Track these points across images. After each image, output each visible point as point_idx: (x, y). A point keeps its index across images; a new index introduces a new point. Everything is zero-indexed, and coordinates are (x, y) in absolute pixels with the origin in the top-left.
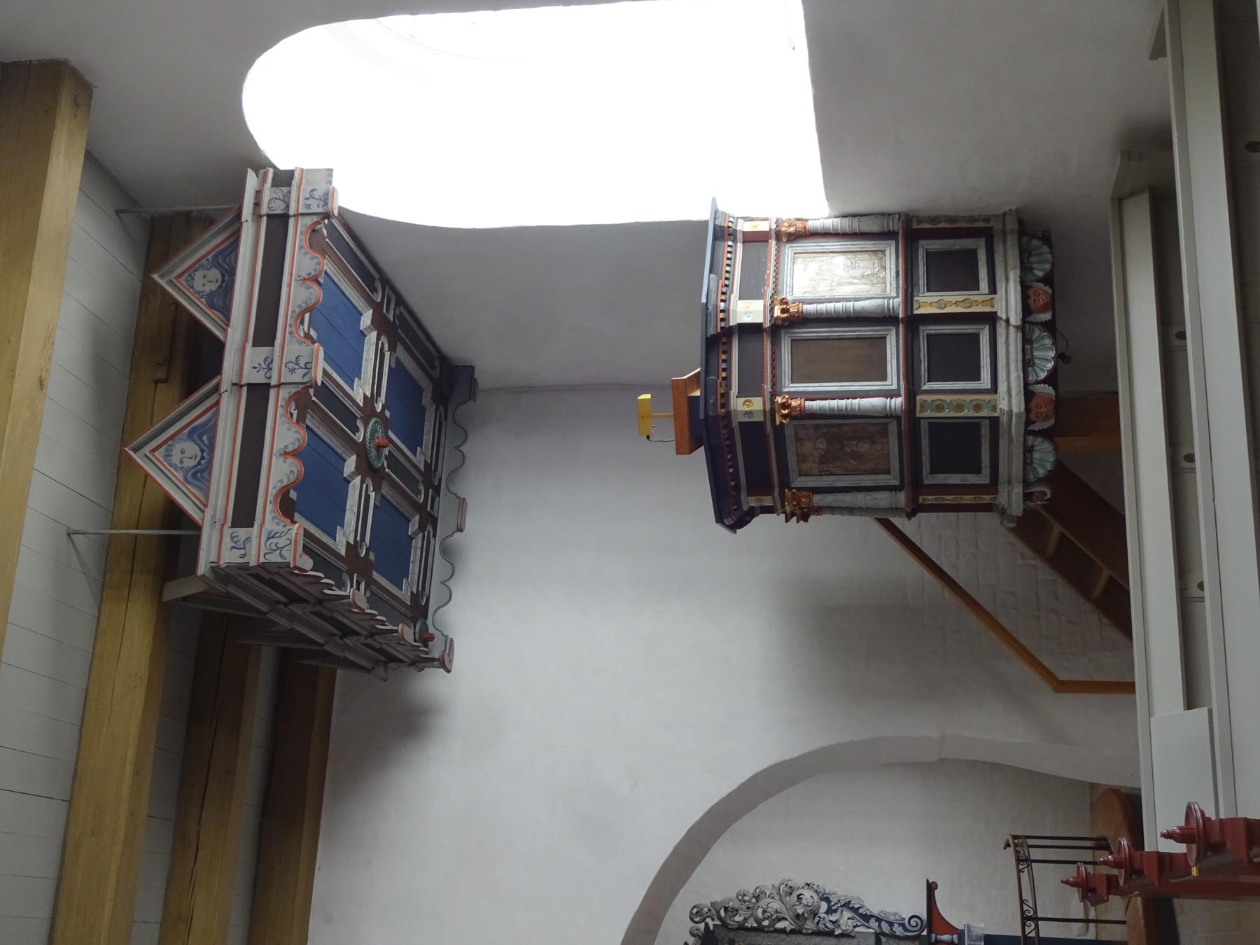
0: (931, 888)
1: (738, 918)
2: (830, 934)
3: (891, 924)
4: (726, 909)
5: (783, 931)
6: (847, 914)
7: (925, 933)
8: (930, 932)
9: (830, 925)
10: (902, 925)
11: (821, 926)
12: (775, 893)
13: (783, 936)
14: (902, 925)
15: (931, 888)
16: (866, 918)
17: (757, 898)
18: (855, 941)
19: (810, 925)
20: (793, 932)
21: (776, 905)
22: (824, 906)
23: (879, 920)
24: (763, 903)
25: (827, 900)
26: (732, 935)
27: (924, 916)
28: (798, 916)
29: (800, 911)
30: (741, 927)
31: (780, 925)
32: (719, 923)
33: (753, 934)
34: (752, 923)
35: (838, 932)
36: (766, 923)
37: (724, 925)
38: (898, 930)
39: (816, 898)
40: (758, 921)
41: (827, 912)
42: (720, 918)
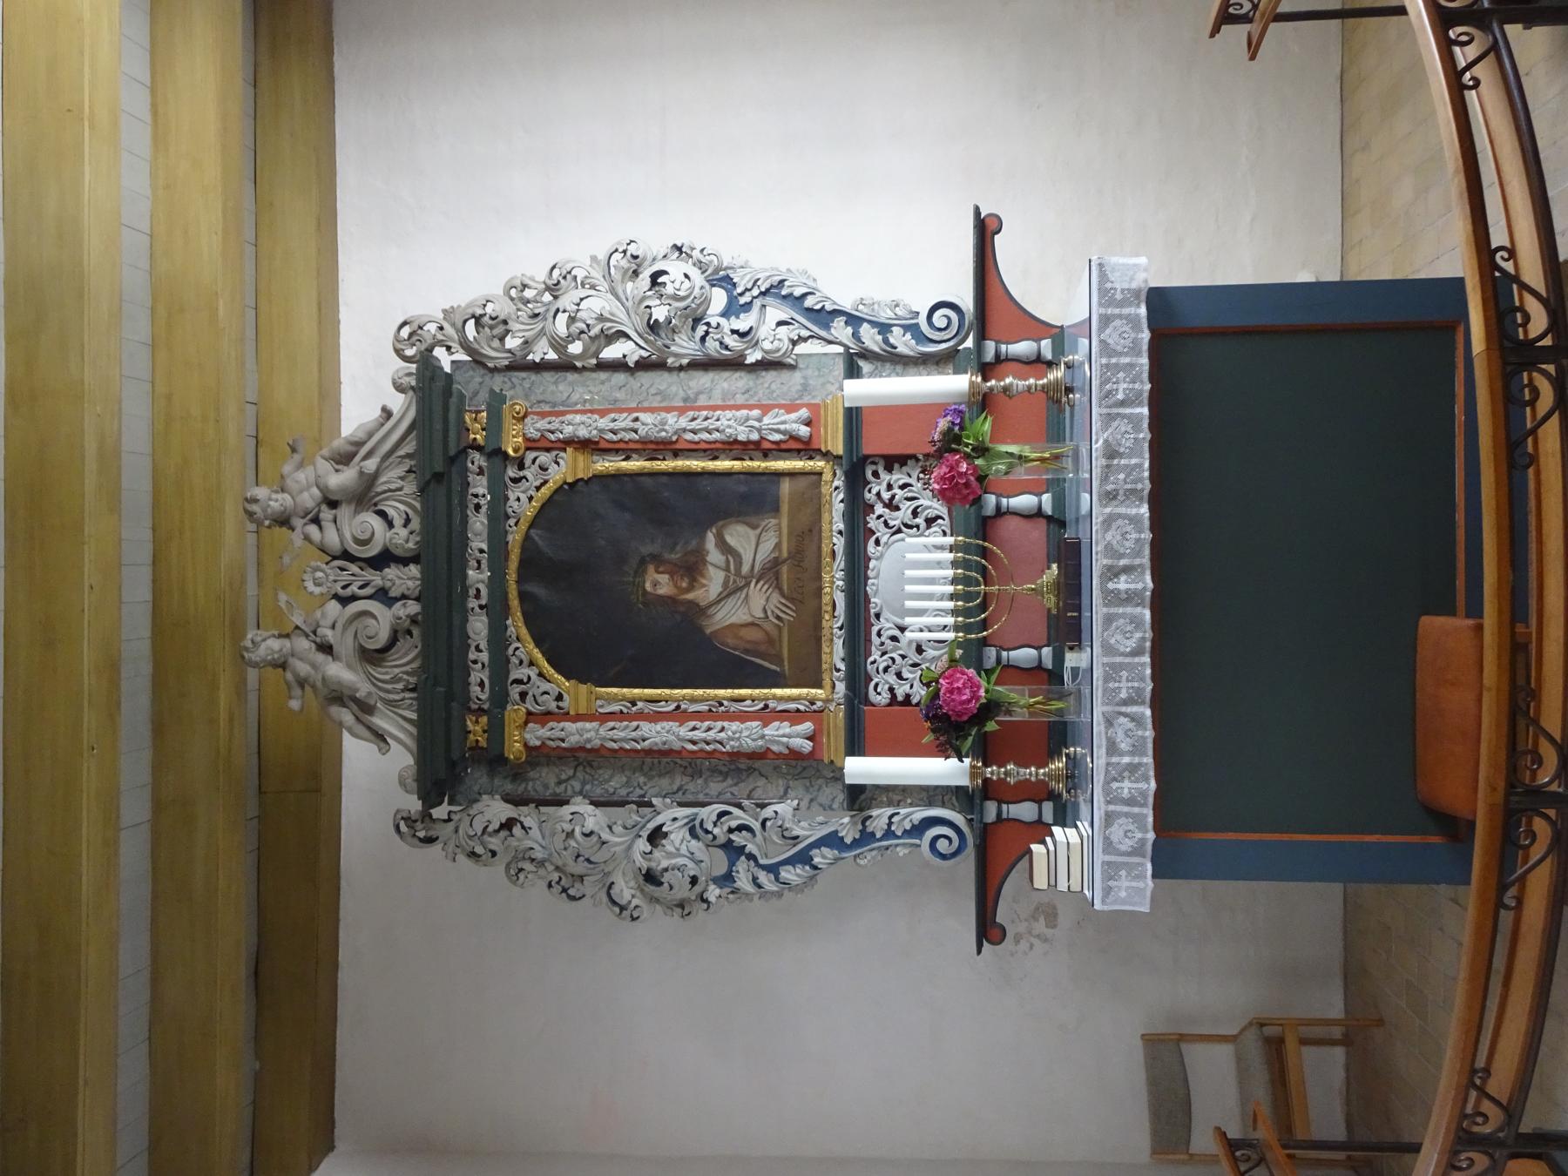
0: (985, 231)
1: (512, 343)
2: (735, 364)
3: (884, 328)
4: (478, 320)
5: (619, 366)
6: (776, 312)
7: (969, 343)
8: (982, 336)
9: (732, 341)
10: (913, 329)
11: (712, 345)
12: (597, 275)
13: (620, 377)
14: (913, 329)
15: (985, 231)
16: (823, 316)
17: (554, 289)
18: (797, 377)
19: (685, 346)
20: (644, 365)
21: (598, 304)
22: (719, 298)
23: (854, 320)
24: (566, 301)
25: (726, 282)
26: (497, 382)
27: (967, 302)
28: (654, 327)
29: (660, 314)
30: (520, 365)
31: (612, 352)
32: (462, 356)
33: (548, 377)
34: (543, 352)
35: (753, 357)
36: (576, 348)
37: (478, 361)
38: (903, 343)
39: (698, 279)
40: (559, 345)
41: (725, 314)
42: (466, 346)
